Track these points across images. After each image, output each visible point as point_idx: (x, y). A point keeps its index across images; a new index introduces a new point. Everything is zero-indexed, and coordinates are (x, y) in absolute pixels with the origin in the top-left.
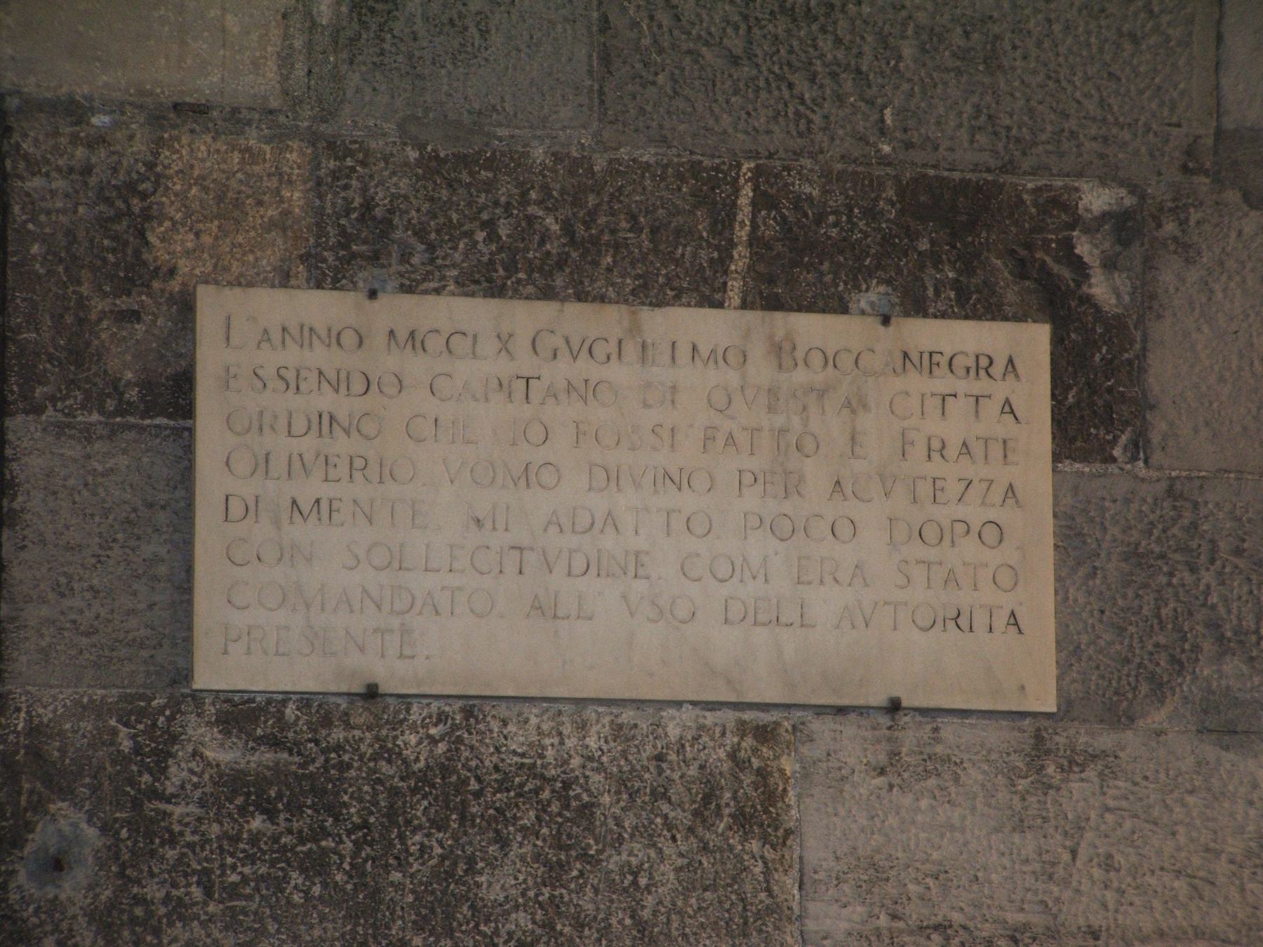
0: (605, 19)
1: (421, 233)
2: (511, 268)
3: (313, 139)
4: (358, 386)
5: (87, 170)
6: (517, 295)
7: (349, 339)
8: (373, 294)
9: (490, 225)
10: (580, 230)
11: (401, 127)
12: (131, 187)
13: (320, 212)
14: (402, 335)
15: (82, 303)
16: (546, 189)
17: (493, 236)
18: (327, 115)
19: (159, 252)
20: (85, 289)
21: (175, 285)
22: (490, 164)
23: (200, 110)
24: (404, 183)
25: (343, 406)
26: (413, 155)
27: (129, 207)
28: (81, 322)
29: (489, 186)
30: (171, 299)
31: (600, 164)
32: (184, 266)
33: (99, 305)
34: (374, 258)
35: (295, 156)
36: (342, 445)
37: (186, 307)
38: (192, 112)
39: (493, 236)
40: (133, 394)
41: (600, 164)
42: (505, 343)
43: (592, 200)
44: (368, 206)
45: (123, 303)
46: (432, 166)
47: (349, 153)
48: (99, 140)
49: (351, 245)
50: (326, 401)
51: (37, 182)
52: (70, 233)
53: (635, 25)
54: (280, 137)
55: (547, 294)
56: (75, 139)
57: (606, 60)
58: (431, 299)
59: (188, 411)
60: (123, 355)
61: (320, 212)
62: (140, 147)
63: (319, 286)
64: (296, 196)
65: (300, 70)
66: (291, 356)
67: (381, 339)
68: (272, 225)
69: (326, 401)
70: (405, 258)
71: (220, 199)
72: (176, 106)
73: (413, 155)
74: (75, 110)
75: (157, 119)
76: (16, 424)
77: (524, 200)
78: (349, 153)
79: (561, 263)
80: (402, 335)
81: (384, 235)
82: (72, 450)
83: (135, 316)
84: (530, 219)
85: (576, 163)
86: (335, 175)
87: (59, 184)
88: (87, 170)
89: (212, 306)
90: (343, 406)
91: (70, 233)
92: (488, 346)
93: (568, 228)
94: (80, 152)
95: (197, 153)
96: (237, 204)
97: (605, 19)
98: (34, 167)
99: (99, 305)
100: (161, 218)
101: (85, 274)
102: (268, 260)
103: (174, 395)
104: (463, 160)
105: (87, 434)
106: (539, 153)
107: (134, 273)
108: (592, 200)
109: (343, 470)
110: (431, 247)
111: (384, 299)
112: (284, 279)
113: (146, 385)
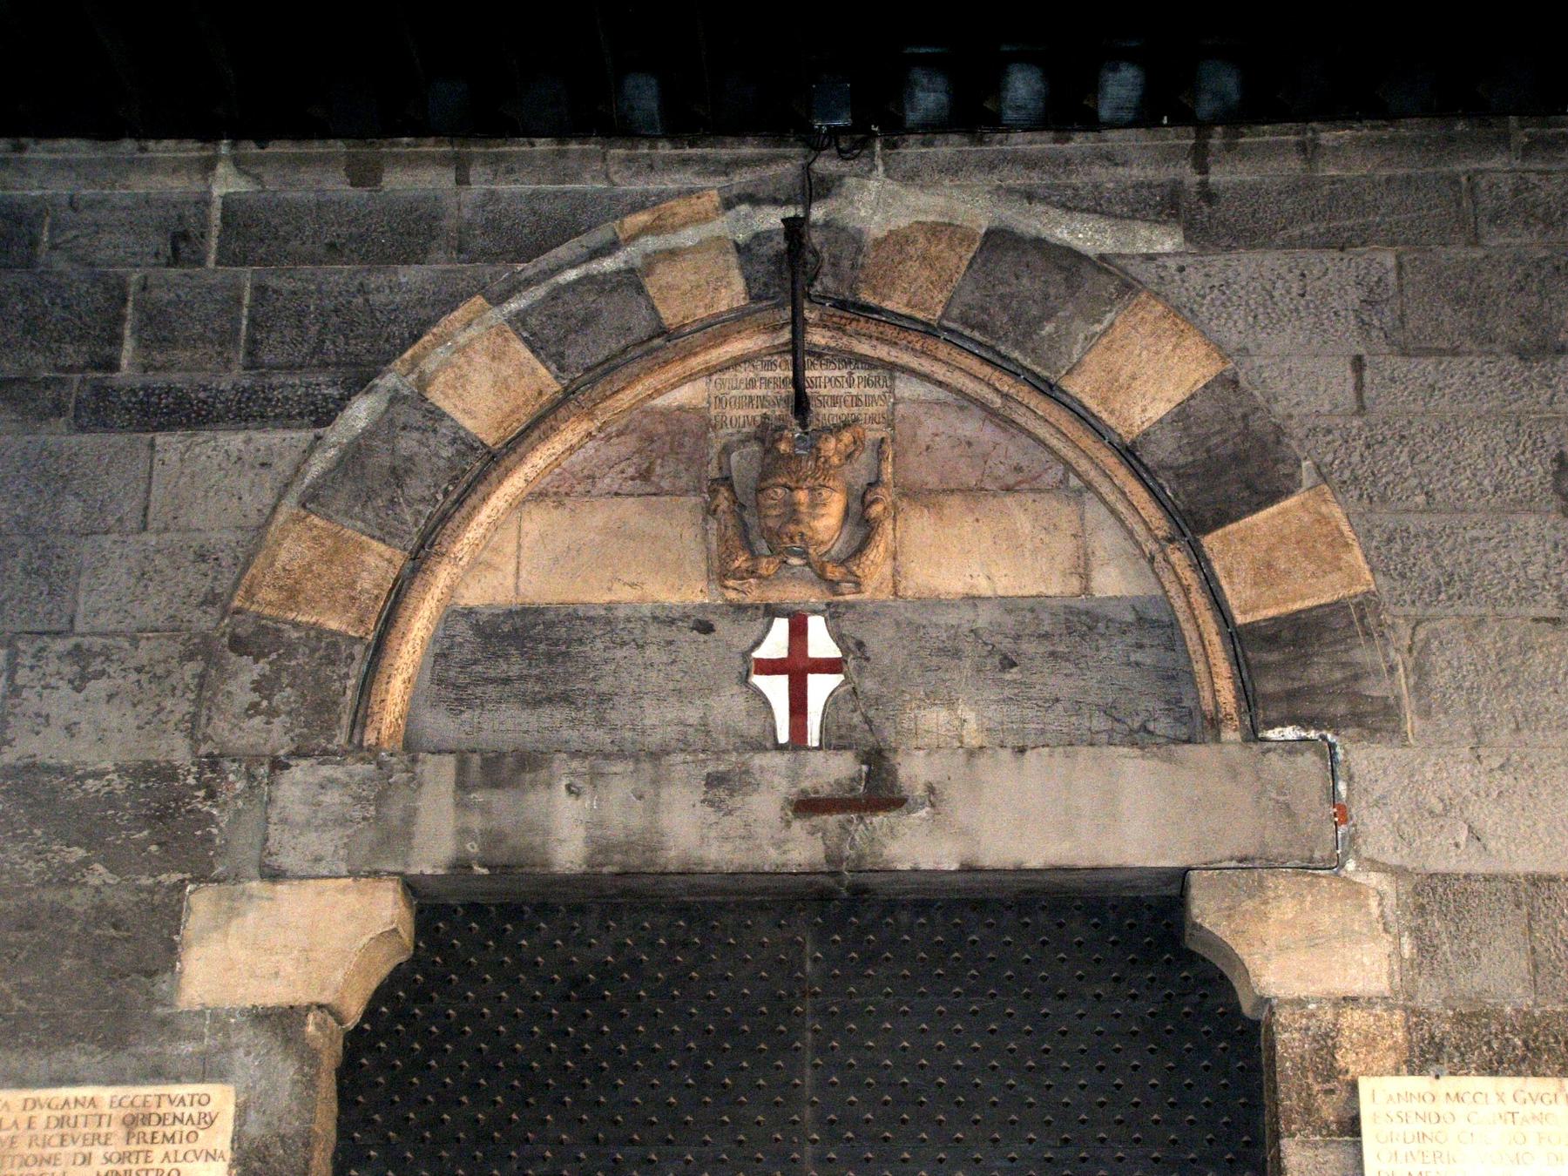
0: (1533, 949)
1: (1457, 1048)
2: (1500, 1062)
3: (1405, 1009)
4: (1434, 1119)
5: (1308, 1029)
6: (1504, 1074)
7: (1428, 1098)
8: (1437, 1077)
9: (1488, 1043)
10: (1532, 1044)
11: (1444, 1001)
12: (1327, 1035)
13: (1411, 1041)
14: (1453, 1095)
15: (1309, 1087)
16: (1513, 1026)
17: (1490, 1048)
18: (1411, 998)
19: (1341, 1063)
20: (1310, 1081)
21: (1349, 1077)
22: (1486, 1015)
23: (1355, 999)
24: (1447, 1027)
25: (1428, 1128)
26: (1451, 1013)
27: (1326, 1042)
28: (1309, 1095)
29: (1487, 1026)
30: (1348, 1083)
31: (1537, 1013)
32: (1352, 1068)
33: (1316, 1088)
34: (1437, 1060)
35: (1398, 1016)
36: (1429, 1147)
37: (1354, 1086)
38: (1351, 1000)
39: (1490, 1048)
40: (1334, 1127)
41: (1537, 1013)
42: (1500, 1096)
43: (1535, 1030)
44: (1432, 1037)
45: (1327, 1086)
46: (1460, 1019)
47: (1421, 1014)
48: (1312, 1015)
49: (1426, 1055)
50: (1421, 1126)
51: (1286, 1035)
52: (1302, 1057)
53: (1547, 950)
54: (1390, 1009)
55: (1518, 1074)
56: (1302, 1016)
57: (1536, 967)
58: (1464, 1078)
59: (1358, 1134)
60: (1328, 1111)
61: (1411, 1041)
62: (1330, 1017)
63: (1413, 1074)
64: (1399, 1035)
65: (1397, 979)
66: (1404, 1107)
67: (1443, 1097)
68: (1389, 1048)
69: (1421, 1126)
70: (1450, 1059)
71: (1366, 1037)
72: (1344, 999)
73: (1451, 1013)
74: (1300, 1003)
75: (1336, 1005)
76: (1284, 1142)
77: (1503, 1032)
78: (1421, 1014)
79: (1524, 1058)
80: (1453, 1095)
81: (1440, 1050)
82: (1310, 1153)
83: (1332, 1091)
84: (1507, 1040)
85: (1526, 1013)
86: (1416, 1024)
87: (1296, 1035)
88: (1308, 1029)
89: (1365, 1085)
90: (1428, 1128)
91: (1302, 1057)
92: (1493, 1098)
93: (1525, 1043)
94: (1304, 1021)
95: (1354, 1018)
96: (1374, 1039)
97: (1533, 949)
98: (1285, 1029)
99: (1316, 1088)
100: (1341, 1047)
101: (1310, 1075)
102: (1389, 1063)
103: (1352, 1126)
104: (1473, 1015)
105: (1315, 1145)
106: (1508, 1009)
107: (1330, 1072)
108: (1535, 1030)
109: (1431, 1158)
110: (1462, 1054)
111: (1442, 1079)
112: (1397, 1072)
113: (1339, 1123)
